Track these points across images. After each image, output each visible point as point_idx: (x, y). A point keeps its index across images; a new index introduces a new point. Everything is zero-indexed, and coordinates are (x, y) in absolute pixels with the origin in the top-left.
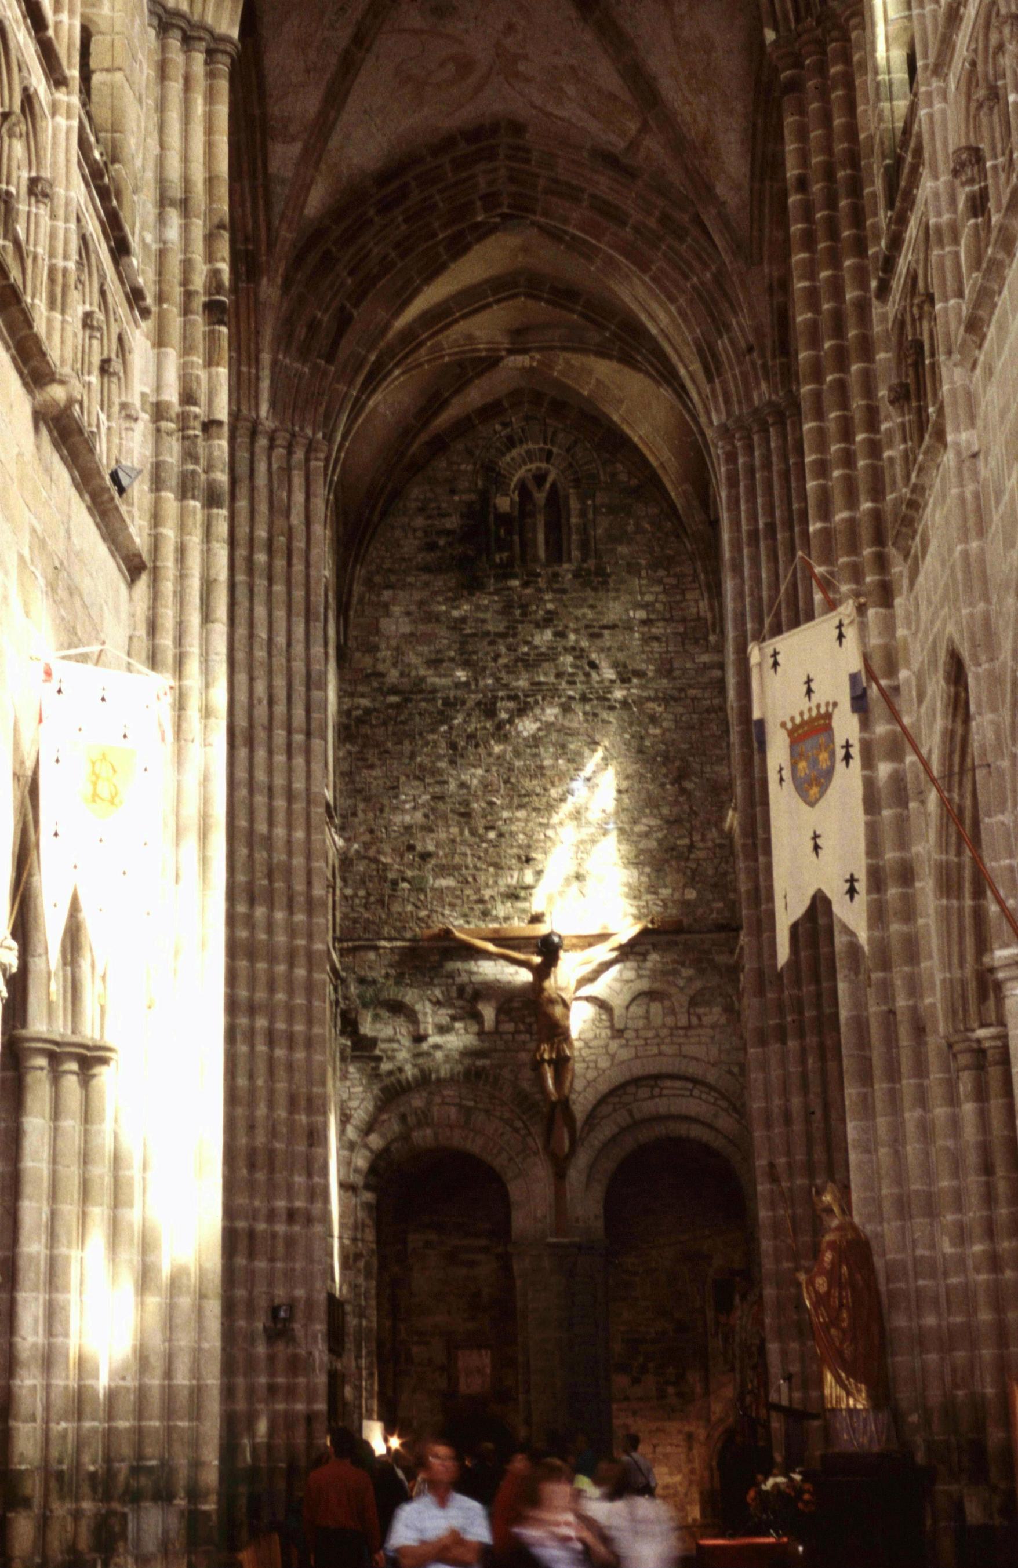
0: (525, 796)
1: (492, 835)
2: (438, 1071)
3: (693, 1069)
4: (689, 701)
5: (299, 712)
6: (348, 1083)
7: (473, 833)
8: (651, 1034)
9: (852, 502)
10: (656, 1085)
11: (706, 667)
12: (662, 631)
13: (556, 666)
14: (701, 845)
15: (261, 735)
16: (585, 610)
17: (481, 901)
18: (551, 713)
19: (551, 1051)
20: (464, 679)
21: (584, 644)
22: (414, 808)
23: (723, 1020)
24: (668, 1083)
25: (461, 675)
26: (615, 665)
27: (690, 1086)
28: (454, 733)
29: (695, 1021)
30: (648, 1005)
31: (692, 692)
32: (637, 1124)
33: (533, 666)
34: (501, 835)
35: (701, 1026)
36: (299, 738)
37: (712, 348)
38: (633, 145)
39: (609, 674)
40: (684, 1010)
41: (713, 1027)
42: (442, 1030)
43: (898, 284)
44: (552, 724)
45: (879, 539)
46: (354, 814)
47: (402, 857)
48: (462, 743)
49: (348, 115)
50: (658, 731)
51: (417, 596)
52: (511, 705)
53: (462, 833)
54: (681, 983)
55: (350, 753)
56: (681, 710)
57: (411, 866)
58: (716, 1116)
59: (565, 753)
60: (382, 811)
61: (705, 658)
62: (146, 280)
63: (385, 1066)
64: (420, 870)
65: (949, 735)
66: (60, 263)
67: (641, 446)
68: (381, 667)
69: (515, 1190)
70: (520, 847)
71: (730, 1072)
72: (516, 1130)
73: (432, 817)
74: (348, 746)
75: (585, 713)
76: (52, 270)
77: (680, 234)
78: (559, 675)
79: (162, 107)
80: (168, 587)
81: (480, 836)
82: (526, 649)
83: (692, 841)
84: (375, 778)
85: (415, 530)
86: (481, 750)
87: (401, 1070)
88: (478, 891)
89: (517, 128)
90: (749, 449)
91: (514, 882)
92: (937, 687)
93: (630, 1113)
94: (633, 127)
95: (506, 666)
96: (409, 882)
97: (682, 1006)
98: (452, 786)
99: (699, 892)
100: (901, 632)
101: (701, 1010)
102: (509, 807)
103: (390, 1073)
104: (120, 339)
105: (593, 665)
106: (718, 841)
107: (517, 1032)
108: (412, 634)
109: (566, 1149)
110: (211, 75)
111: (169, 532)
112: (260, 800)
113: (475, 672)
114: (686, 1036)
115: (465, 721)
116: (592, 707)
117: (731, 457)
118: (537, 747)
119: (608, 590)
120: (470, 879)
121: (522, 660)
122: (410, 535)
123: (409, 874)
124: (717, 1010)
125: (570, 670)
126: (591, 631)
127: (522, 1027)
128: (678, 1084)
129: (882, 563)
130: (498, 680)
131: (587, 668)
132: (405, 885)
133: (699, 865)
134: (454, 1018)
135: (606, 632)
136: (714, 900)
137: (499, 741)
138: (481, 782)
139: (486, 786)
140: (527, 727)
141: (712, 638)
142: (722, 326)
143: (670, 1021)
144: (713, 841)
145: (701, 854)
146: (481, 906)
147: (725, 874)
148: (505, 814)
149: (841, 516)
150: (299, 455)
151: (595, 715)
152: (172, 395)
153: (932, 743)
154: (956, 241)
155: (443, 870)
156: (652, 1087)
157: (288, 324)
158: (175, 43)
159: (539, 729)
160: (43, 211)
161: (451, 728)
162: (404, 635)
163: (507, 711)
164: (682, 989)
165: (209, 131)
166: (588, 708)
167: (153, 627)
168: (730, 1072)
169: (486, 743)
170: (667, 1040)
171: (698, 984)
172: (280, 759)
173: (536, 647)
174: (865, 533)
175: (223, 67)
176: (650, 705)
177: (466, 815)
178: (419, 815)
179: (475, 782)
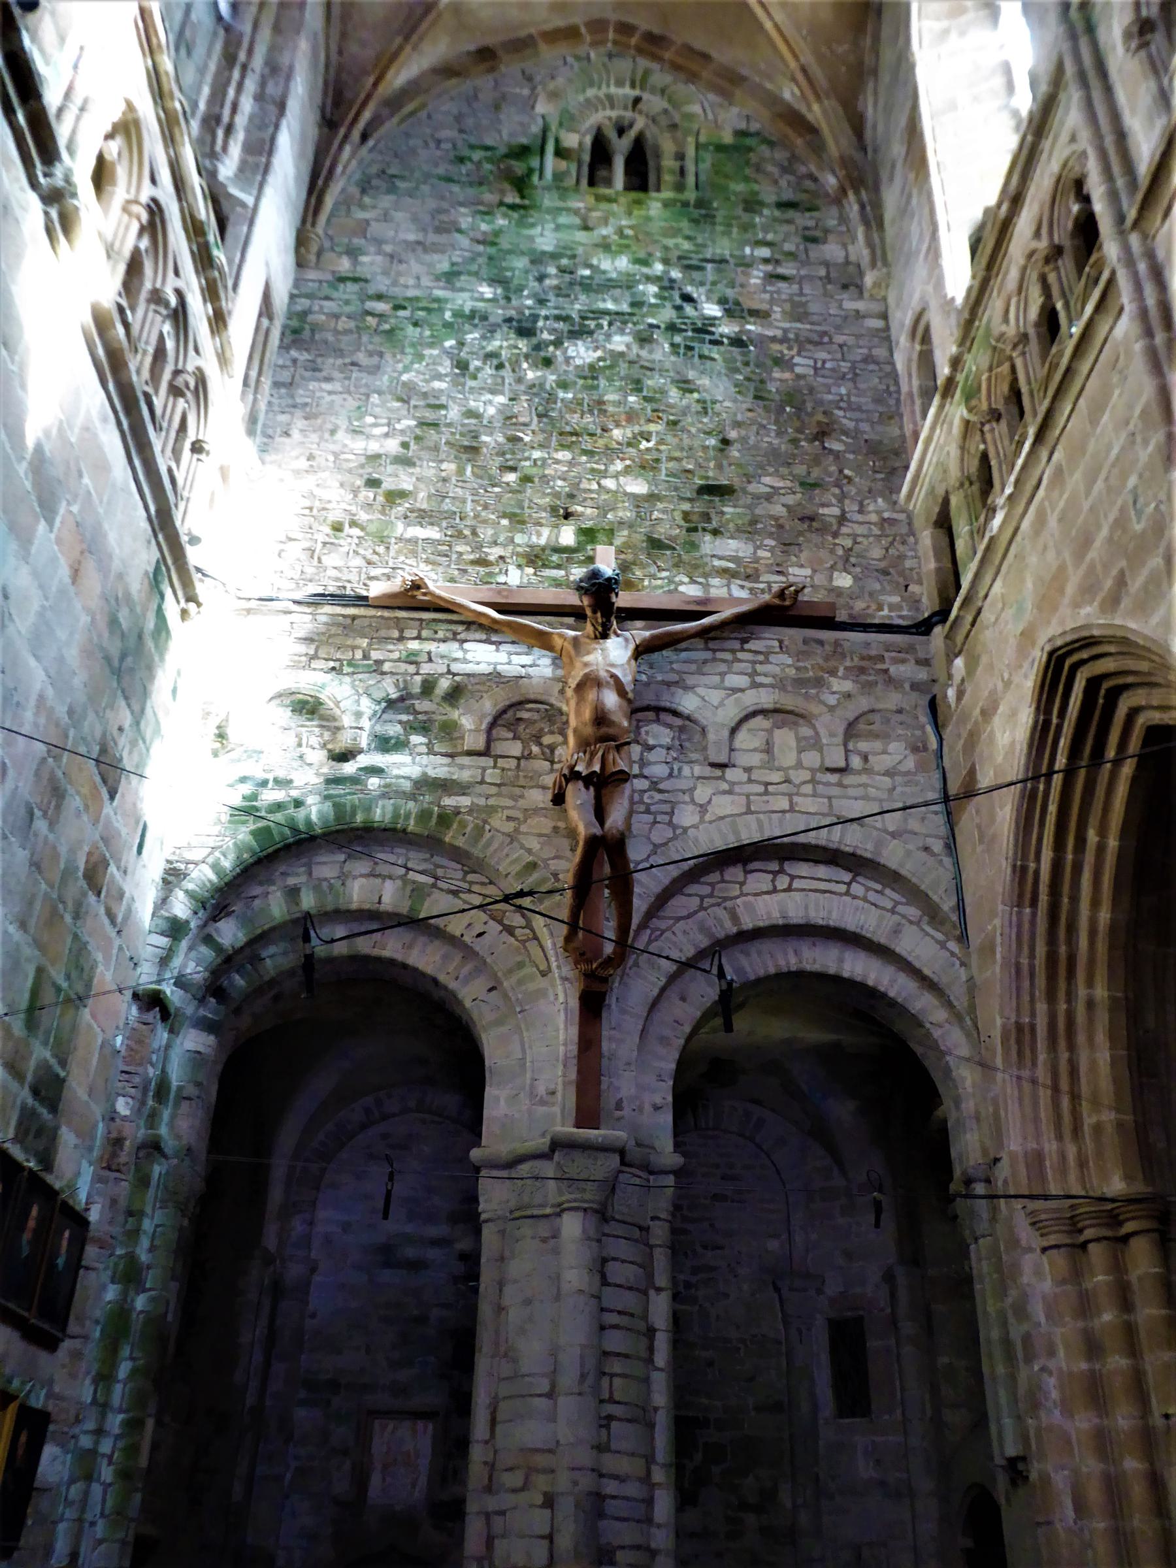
0: (572, 434)
1: (511, 477)
2: (368, 809)
4: (835, 347)
7: (482, 473)
8: (776, 777)
10: (782, 871)
12: (794, 272)
13: (633, 295)
14: (860, 518)
16: (680, 240)
17: (482, 562)
18: (620, 342)
19: (590, 763)
20: (489, 296)
21: (676, 274)
22: (387, 435)
23: (910, 764)
24: (803, 869)
25: (487, 291)
26: (722, 301)
27: (847, 876)
28: (466, 349)
29: (856, 762)
30: (770, 732)
31: (839, 339)
33: (597, 292)
34: (527, 479)
35: (866, 771)
39: (712, 310)
40: (840, 739)
41: (888, 773)
42: (385, 744)
44: (622, 354)
46: (287, 434)
47: (355, 492)
48: (477, 363)
50: (787, 375)
51: (432, 204)
52: (560, 325)
53: (461, 471)
54: (832, 700)
55: (295, 361)
56: (822, 355)
57: (368, 506)
58: (897, 931)
59: (640, 390)
60: (333, 432)
61: (860, 305)
63: (271, 795)
64: (383, 513)
67: (774, 34)
68: (361, 271)
70: (556, 495)
71: (926, 849)
72: (510, 930)
73: (413, 446)
74: (294, 353)
75: (672, 345)
78: (633, 304)
81: (491, 477)
82: (587, 272)
83: (844, 512)
84: (330, 393)
85: (439, 142)
86: (507, 373)
88: (479, 547)
91: (543, 541)
93: (735, 918)
95: (558, 288)
96: (363, 529)
97: (832, 735)
98: (454, 413)
99: (856, 579)
101: (863, 746)
102: (542, 446)
103: (278, 807)
105: (687, 298)
106: (886, 515)
107: (529, 756)
108: (419, 243)
109: (609, 949)
113: (507, 289)
114: (840, 784)
115: (484, 337)
116: (685, 338)
118: (594, 378)
119: (714, 224)
120: (467, 532)
121: (581, 284)
122: (432, 145)
123: (363, 516)
124: (897, 749)
125: (653, 301)
126: (686, 262)
127: (535, 749)
128: (822, 871)
130: (542, 302)
131: (678, 301)
132: (356, 532)
133: (855, 543)
134: (410, 728)
135: (709, 266)
136: (883, 591)
137: (534, 366)
138: (500, 411)
139: (509, 418)
140: (582, 353)
141: (869, 279)
143: (812, 758)
144: (878, 512)
145: (860, 530)
146: (482, 570)
147: (902, 557)
148: (537, 454)
151: (691, 348)
156: (775, 873)
159: (600, 359)
161: (461, 344)
162: (405, 241)
163: (552, 331)
164: (832, 709)
166: (678, 339)
168: (926, 849)
169: (515, 365)
170: (808, 789)
171: (864, 703)
173: (604, 272)
176: (776, 347)
177: (473, 450)
178: (392, 446)
179: (491, 411)
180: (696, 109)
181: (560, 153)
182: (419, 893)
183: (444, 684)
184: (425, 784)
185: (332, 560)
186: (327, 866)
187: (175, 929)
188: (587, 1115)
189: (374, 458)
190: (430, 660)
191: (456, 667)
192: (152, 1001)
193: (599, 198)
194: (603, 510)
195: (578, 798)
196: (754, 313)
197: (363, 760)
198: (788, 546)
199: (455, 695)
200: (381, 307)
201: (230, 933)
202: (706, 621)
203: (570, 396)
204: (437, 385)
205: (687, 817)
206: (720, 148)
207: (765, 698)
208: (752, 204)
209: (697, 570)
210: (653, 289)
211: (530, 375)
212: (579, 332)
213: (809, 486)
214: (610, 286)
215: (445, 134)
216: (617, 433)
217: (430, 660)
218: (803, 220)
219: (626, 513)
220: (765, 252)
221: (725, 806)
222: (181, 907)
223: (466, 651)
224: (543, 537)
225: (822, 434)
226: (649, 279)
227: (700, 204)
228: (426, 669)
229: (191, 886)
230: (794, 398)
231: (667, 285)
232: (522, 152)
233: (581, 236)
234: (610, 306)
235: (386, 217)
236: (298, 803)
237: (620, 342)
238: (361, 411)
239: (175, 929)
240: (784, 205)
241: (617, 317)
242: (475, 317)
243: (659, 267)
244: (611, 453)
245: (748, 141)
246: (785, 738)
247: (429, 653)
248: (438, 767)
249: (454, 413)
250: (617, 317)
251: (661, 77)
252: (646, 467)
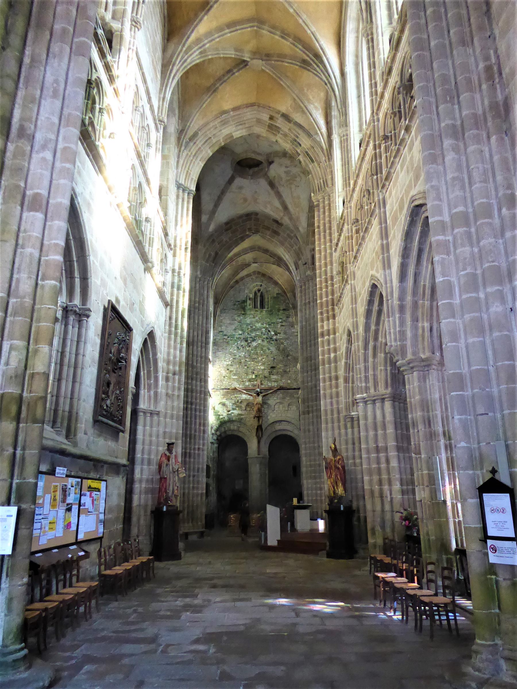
3: (288, 419)
5: (204, 339)
9: (327, 296)
11: (294, 332)
15: (195, 344)
18: (260, 341)
25: (240, 332)
32: (276, 431)
36: (204, 344)
37: (297, 263)
38: (282, 218)
39: (273, 333)
42: (233, 409)
43: (339, 249)
45: (333, 305)
49: (220, 208)
62: (172, 243)
63: (221, 417)
65: (347, 348)
66: (152, 236)
68: (223, 330)
69: (249, 445)
76: (150, 238)
77: (291, 238)
79: (177, 204)
80: (174, 310)
89: (256, 214)
90: (305, 285)
92: (345, 337)
94: (282, 214)
98: (237, 356)
100: (337, 325)
104: (165, 255)
110: (188, 198)
111: (175, 297)
112: (195, 358)
117: (301, 287)
129: (333, 309)
139: (245, 356)
140: (254, 344)
142: (300, 259)
149: (324, 299)
150: (206, 283)
152: (177, 268)
153: (343, 349)
154: (352, 239)
155: (235, 375)
157: (205, 253)
158: (181, 191)
160: (149, 225)
165: (188, 210)
167: (170, 318)
171: (290, 401)
172: (200, 349)
174: (330, 303)
175: (191, 197)
178: (230, 363)
180: (270, 289)
181: (250, 299)
182: (239, 427)
184: (239, 415)
185: (224, 382)
186: (228, 425)
187: (213, 434)
188: (259, 454)
189: (228, 365)
192: (212, 443)
193: (256, 311)
194: (258, 372)
195: (256, 419)
196: (280, 333)
198: (282, 376)
199: (241, 402)
200: (226, 337)
201: (218, 433)
202: (271, 391)
205: (269, 417)
206: (274, 298)
207: (278, 401)
208: (279, 310)
209: (270, 380)
212: (254, 340)
213: (286, 366)
214: (258, 329)
215: (232, 299)
216: (260, 358)
218: (287, 313)
219: (261, 372)
220: (280, 320)
221: (274, 416)
222: (213, 432)
224: (250, 377)
225: (288, 356)
226: (264, 328)
227: (271, 311)
230: (284, 350)
231: (266, 329)
232: (244, 302)
233: (253, 320)
235: (224, 318)
237: (260, 341)
238: (225, 357)
239: (213, 434)
240: (284, 310)
241: (260, 337)
242: (239, 338)
244: (258, 362)
245: (279, 296)
246: (281, 406)
248: (240, 412)
249: (237, 356)
250: (260, 337)
251: (265, 282)
252: (263, 364)
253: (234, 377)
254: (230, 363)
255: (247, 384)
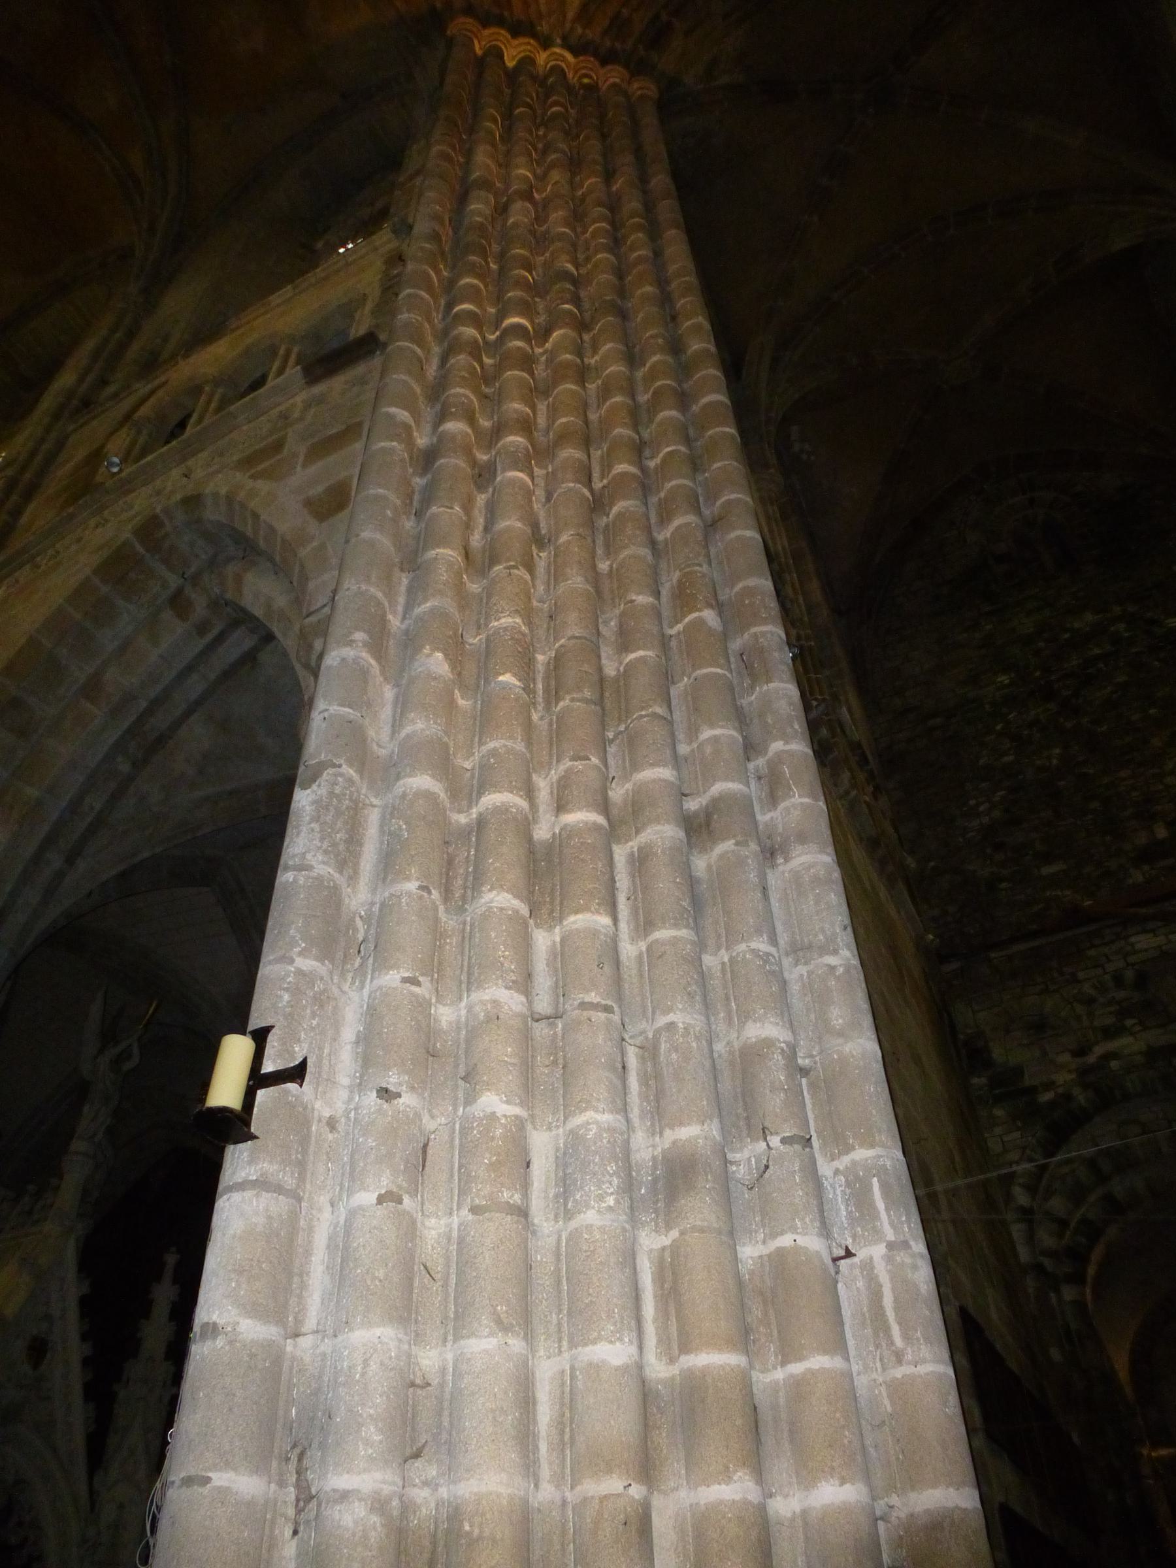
1: (1095, 805)
6: (998, 1130)
25: (1004, 679)
42: (1109, 1033)
82: (1067, 636)
87: (1068, 1097)
132: (1004, 885)
179: (1055, 762)
183: (1130, 974)
184: (1152, 1054)
190: (1109, 961)
191: (1131, 959)
197: (1098, 1050)
203: (1105, 727)
204: (1006, 759)
210: (1121, 626)
211: (1069, 725)
217: (1109, 961)
223: (1132, 945)
224: (1142, 839)
228: (1110, 967)
229: (1021, 1181)
234: (1097, 651)
236: (1068, 1097)
243: (1117, 610)
247: (1107, 956)
253: (1046, 870)
254: (997, 814)
255: (1137, 876)
